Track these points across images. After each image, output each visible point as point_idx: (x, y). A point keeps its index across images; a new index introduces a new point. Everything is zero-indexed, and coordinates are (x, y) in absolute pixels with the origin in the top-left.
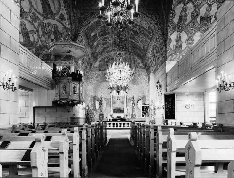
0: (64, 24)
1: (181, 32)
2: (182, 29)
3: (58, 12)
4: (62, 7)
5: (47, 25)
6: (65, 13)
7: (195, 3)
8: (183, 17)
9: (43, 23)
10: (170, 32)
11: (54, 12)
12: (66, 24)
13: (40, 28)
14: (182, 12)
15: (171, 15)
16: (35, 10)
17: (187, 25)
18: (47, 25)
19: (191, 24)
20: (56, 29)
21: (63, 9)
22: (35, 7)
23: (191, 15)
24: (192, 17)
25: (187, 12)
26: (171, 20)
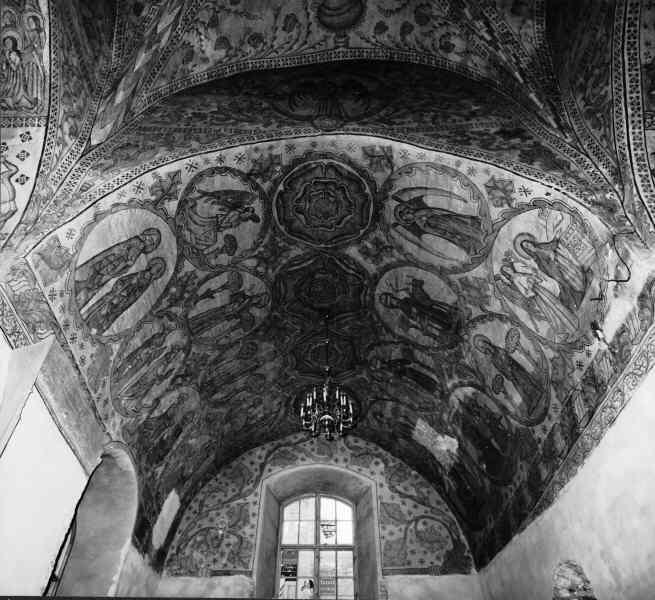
0: (527, 199)
3: (479, 197)
4: (463, 169)
5: (510, 271)
6: (487, 172)
9: (497, 278)
11: (473, 208)
12: (526, 192)
13: (510, 304)
16: (455, 270)
18: (510, 271)
20: (533, 249)
21: (472, 171)
22: (447, 264)
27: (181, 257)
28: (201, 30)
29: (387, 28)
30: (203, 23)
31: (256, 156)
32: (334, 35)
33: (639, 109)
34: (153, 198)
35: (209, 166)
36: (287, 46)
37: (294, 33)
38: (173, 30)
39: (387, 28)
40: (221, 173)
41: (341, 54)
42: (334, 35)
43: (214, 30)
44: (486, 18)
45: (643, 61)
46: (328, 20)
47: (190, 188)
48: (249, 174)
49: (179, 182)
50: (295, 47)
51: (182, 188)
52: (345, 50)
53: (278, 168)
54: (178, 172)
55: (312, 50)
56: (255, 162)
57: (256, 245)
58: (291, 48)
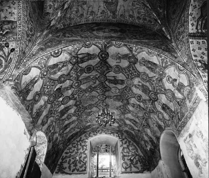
1: (42, 78)
2: (46, 75)
7: (72, 71)
8: (57, 68)
10: (37, 63)
14: (62, 62)
15: (56, 52)
17: (51, 79)
19: (52, 82)
23: (61, 75)
24: (60, 77)
25: (63, 69)
26: (51, 55)
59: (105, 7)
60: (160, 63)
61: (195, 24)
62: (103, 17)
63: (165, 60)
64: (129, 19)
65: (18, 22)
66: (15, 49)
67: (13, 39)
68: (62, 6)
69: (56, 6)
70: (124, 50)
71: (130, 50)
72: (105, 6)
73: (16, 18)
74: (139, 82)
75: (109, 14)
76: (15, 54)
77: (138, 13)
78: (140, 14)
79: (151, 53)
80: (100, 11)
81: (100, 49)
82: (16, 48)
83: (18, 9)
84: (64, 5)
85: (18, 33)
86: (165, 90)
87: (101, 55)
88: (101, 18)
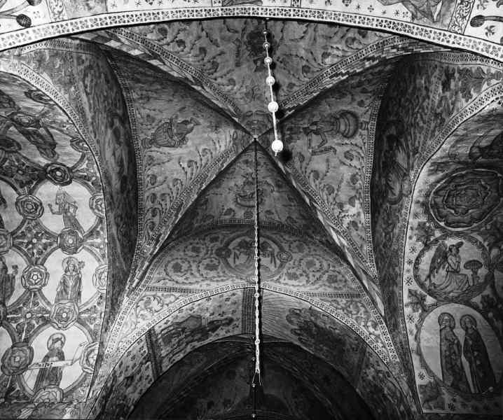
27: (468, 303)
28: (343, 214)
29: (362, 101)
30: (340, 212)
31: (415, 238)
32: (360, 130)
33: (444, 35)
34: (420, 311)
35: (412, 270)
36: (361, 160)
37: (354, 153)
38: (340, 234)
39: (362, 101)
40: (418, 264)
41: (372, 126)
42: (360, 130)
43: (345, 206)
44: (364, 59)
45: (409, 20)
46: (350, 134)
47: (422, 285)
48: (426, 245)
49: (416, 292)
50: (363, 155)
51: (420, 290)
52: (370, 124)
53: (427, 224)
54: (410, 291)
55: (366, 144)
56: (418, 240)
57: (481, 246)
58: (363, 157)
59: (161, 121)
60: (85, 305)
61: (169, 323)
62: (142, 121)
63: (95, 315)
64: (148, 176)
65: (107, 16)
66: (29, 30)
67: (58, 9)
68: (153, 53)
69: (149, 36)
70: (87, 219)
71: (93, 233)
72: (163, 122)
73: (115, 10)
74: (15, 267)
75: (150, 133)
76: (14, 34)
77: (164, 194)
78: (163, 200)
79: (100, 278)
80: (152, 114)
81: (74, 168)
82: (34, 31)
83: (138, 13)
84: (156, 57)
85: (78, 20)
86: (27, 341)
87: (58, 169)
88: (139, 116)
